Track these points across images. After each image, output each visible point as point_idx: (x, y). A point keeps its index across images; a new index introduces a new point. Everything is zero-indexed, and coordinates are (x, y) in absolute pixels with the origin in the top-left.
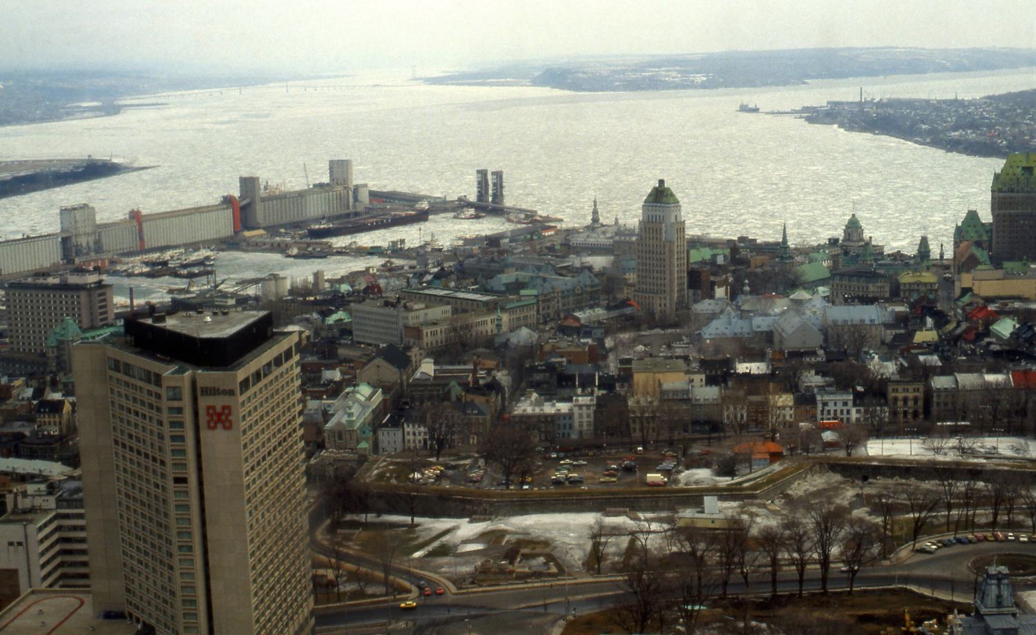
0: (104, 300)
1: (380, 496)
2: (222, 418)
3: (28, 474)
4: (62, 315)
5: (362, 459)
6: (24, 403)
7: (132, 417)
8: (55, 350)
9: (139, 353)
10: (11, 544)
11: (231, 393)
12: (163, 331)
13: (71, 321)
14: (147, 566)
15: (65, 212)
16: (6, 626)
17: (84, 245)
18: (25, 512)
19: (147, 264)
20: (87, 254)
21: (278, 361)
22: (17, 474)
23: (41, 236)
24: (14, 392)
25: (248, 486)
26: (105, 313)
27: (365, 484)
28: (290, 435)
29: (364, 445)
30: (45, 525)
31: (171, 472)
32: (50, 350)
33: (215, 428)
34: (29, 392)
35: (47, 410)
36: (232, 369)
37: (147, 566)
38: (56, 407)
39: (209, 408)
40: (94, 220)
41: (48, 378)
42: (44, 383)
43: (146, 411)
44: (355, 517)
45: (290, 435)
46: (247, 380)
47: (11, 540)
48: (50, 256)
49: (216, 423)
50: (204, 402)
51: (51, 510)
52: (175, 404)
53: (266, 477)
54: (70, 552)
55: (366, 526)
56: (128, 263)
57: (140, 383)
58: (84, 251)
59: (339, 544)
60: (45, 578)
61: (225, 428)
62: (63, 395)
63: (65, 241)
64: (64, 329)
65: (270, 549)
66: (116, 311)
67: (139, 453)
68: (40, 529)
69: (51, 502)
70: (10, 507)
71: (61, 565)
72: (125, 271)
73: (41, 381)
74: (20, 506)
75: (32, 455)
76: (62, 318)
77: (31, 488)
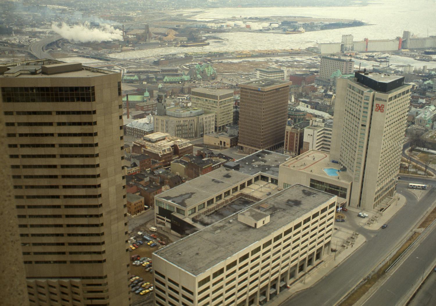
0: (351, 66)
1: (430, 143)
2: (381, 108)
5: (427, 130)
7: (352, 103)
9: (358, 84)
10: (309, 135)
11: (386, 101)
12: (367, 78)
14: (348, 149)
17: (348, 47)
18: (314, 126)
19: (367, 56)
21: (403, 93)
25: (385, 132)
26: (351, 70)
27: (425, 138)
28: (403, 118)
29: (428, 126)
30: (320, 131)
31: (361, 122)
33: (378, 111)
34: (323, 91)
36: (387, 93)
37: (348, 149)
38: (330, 96)
39: (377, 104)
40: (352, 40)
41: (329, 87)
42: (328, 89)
43: (357, 102)
44: (419, 148)
45: (403, 118)
46: (391, 98)
48: (336, 50)
49: (378, 110)
50: (376, 102)
52: (367, 101)
53: (392, 130)
55: (423, 152)
57: (357, 93)
59: (412, 156)
60: (317, 147)
61: (381, 112)
63: (342, 45)
65: (388, 152)
67: (352, 114)
68: (318, 132)
69: (323, 125)
70: (310, 124)
71: (323, 144)
75: (320, 110)
77: (318, 119)
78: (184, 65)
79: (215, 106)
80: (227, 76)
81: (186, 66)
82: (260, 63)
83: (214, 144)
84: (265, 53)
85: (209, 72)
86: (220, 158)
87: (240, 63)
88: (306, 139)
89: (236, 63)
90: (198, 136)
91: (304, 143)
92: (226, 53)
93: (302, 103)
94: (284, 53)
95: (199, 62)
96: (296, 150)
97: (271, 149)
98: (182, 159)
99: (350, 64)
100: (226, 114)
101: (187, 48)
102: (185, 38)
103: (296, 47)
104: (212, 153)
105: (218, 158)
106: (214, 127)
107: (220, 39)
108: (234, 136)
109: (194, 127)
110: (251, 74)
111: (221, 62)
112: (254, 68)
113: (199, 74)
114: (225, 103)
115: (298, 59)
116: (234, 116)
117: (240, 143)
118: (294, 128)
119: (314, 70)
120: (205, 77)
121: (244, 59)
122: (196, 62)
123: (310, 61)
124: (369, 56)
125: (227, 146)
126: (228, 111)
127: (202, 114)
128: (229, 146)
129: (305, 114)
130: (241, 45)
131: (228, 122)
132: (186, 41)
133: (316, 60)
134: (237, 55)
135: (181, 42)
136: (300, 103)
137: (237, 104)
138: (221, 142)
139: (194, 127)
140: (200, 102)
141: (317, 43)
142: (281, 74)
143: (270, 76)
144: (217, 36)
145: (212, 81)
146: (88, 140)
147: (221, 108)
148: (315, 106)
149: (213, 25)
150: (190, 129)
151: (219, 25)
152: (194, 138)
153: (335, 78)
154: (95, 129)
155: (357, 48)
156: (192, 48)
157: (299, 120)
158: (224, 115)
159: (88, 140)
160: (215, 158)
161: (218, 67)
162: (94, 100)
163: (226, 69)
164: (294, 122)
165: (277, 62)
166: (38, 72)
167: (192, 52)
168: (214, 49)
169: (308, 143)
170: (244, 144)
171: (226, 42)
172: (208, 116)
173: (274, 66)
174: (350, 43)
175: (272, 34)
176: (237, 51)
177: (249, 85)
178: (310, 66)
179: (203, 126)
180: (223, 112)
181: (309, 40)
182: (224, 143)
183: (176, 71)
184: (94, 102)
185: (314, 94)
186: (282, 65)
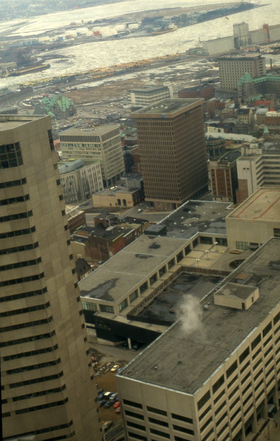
0: (262, 64)
3: (238, 140)
4: (243, 71)
6: (232, 110)
8: (241, 87)
10: (244, 169)
13: (248, 74)
15: (235, 26)
16: (253, 202)
17: (244, 41)
18: (249, 155)
19: (272, 48)
20: (245, 45)
22: (233, 140)
23: (225, 38)
24: (226, 106)
26: (262, 70)
30: (258, 162)
32: (239, 87)
34: (233, 105)
35: (242, 113)
38: (246, 112)
40: (248, 29)
41: (240, 100)
42: (238, 101)
47: (244, 167)
48: (229, 47)
51: (260, 154)
54: (268, 173)
56: (263, 48)
58: (244, 43)
62: (248, 107)
63: (236, 39)
64: (245, 78)
66: (266, 69)
68: (257, 163)
69: (260, 151)
70: (243, 152)
72: (263, 52)
73: (236, 101)
74: (247, 153)
75: (238, 132)
76: (243, 73)
78: (24, 102)
79: (97, 151)
80: (89, 107)
81: (27, 102)
82: (129, 81)
83: (110, 206)
84: (132, 66)
85: (64, 106)
86: (130, 223)
87: (102, 85)
88: (241, 175)
89: (96, 87)
90: (83, 198)
91: (239, 182)
92: (77, 75)
93: (211, 127)
94: (159, 62)
95: (44, 94)
96: (229, 194)
97: (195, 197)
98: (76, 235)
99: (260, 62)
100: (115, 160)
101: (20, 77)
102: (13, 64)
103: (173, 52)
104: (116, 219)
105: (127, 224)
106: (101, 181)
107: (63, 57)
108: (136, 189)
109: (74, 186)
110: (122, 100)
111: (75, 89)
112: (124, 89)
113: (50, 110)
114: (111, 145)
115: (180, 67)
116: (125, 161)
117: (148, 197)
119: (207, 79)
120: (59, 114)
121: (105, 80)
122: (39, 94)
123: (197, 68)
124: (275, 48)
125: (128, 205)
126: (117, 155)
127: (82, 166)
128: (132, 205)
129: (223, 142)
130: (94, 60)
131: (119, 170)
132: (15, 67)
133: (205, 65)
134: (93, 75)
135: (9, 69)
136: (208, 128)
137: (127, 144)
138: (119, 201)
139: (74, 186)
140: (74, 149)
141: (200, 42)
142: (165, 93)
143: (151, 97)
144: (57, 54)
145: (71, 118)
146: (20, 225)
147: (106, 152)
148: (230, 129)
149: (47, 38)
150: (70, 190)
151: (56, 37)
152: (78, 202)
153: (243, 85)
154: (29, 205)
155: (255, 39)
156: (28, 75)
157: (217, 151)
158: (112, 162)
159: (20, 225)
160: (123, 225)
161: (73, 97)
162: (21, 163)
163: (84, 99)
164: (211, 156)
165: (152, 76)
167: (29, 82)
168: (58, 73)
169: (245, 181)
170: (154, 198)
171: (73, 60)
172: (91, 166)
173: (153, 83)
174: (246, 34)
175: (134, 39)
176: (92, 71)
177: (148, 113)
178: (201, 74)
179: (87, 183)
180: (111, 158)
181: (186, 39)
182: (124, 201)
183: (15, 111)
184: (21, 166)
185: (223, 112)
186: (161, 78)
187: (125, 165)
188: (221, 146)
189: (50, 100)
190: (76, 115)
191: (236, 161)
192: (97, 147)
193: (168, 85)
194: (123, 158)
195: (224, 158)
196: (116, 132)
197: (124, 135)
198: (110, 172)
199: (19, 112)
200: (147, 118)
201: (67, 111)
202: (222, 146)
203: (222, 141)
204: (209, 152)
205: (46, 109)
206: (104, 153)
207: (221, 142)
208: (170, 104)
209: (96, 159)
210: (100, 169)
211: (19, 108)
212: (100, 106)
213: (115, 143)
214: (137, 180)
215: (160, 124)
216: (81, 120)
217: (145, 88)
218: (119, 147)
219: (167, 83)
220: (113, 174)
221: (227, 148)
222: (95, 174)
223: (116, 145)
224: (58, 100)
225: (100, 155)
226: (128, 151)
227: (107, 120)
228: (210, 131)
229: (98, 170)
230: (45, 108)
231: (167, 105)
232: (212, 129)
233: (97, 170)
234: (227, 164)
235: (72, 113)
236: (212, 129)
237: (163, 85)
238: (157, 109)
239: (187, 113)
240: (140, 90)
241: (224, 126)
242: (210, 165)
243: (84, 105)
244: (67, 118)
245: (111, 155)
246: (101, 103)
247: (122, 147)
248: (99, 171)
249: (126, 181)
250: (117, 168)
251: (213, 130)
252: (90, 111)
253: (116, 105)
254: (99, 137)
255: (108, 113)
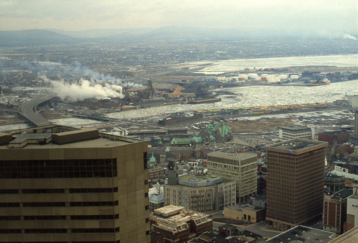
10: (353, 206)
16: (351, 236)
78: (194, 125)
79: (236, 172)
80: (244, 136)
81: (196, 125)
82: (281, 120)
83: (237, 219)
84: (286, 108)
85: (223, 132)
86: (246, 236)
87: (259, 120)
88: (350, 211)
89: (253, 121)
90: (217, 209)
91: (347, 216)
92: (241, 110)
93: (338, 167)
94: (308, 107)
95: (211, 121)
96: (338, 225)
97: (308, 224)
98: (201, 238)
100: (249, 182)
102: (193, 94)
103: (322, 101)
104: (237, 230)
105: (244, 236)
106: (235, 197)
107: (233, 94)
108: (261, 208)
109: (211, 198)
110: (272, 134)
111: (237, 120)
112: (275, 126)
113: (212, 134)
114: (248, 170)
116: (258, 184)
117: (269, 217)
118: (334, 197)
119: (346, 126)
120: (218, 138)
121: (262, 117)
122: (207, 121)
123: (340, 116)
125: (252, 221)
126: (252, 178)
127: (220, 183)
128: (255, 221)
129: (343, 179)
130: (257, 100)
131: (252, 191)
132: (194, 97)
133: (347, 115)
134: (254, 112)
135: (188, 98)
136: (336, 166)
137: (261, 170)
138: (245, 216)
139: (211, 198)
140: (218, 168)
141: (346, 96)
142: (307, 133)
143: (295, 135)
144: (229, 91)
145: (227, 143)
146: (107, 224)
147: (242, 175)
149: (224, 78)
150: (207, 201)
151: (231, 78)
152: (212, 211)
154: (116, 210)
157: (337, 187)
158: (247, 183)
159: (107, 224)
160: (240, 236)
162: (116, 175)
164: (331, 190)
165: (301, 118)
166: (48, 141)
168: (226, 106)
170: (273, 218)
171: (240, 97)
172: (228, 184)
173: (299, 123)
175: (292, 87)
176: (253, 107)
177: (278, 147)
178: (341, 122)
179: (223, 197)
181: (336, 92)
182: (249, 217)
183: (185, 131)
184: (114, 178)
185: (351, 155)
186: (308, 120)
187: (257, 187)
188: (341, 183)
189: (214, 126)
190: (232, 141)
191: (347, 199)
192: (236, 169)
193: (311, 127)
194: (256, 181)
195: (337, 194)
196: (254, 159)
197: (262, 163)
198: (243, 191)
199: (188, 132)
200: (276, 152)
201: (225, 136)
202: (342, 184)
203: (342, 179)
204: (330, 186)
205: (209, 133)
206: (241, 175)
207: (342, 180)
208: (298, 143)
209: (234, 179)
210: (235, 187)
211: (189, 129)
212: (253, 136)
213: (251, 169)
214: (263, 201)
215: (287, 158)
216: (235, 146)
217: (292, 127)
218: (254, 172)
219: (311, 125)
220: (246, 193)
221: (346, 186)
222: (231, 191)
223: (252, 170)
224: (219, 127)
225: (238, 176)
226: (262, 176)
227: (256, 148)
228: (337, 170)
229: (230, 189)
230: (209, 132)
231: (295, 143)
232: (338, 168)
233: (232, 188)
234: (339, 199)
235: (229, 139)
236: (338, 168)
237: (307, 127)
238: (287, 145)
239: (311, 153)
240: (287, 128)
241: (349, 167)
242: (325, 198)
243: (241, 133)
244: (224, 142)
245: (246, 177)
246: (254, 134)
247: (258, 173)
248: (234, 189)
249: (254, 201)
250: (250, 189)
251: (339, 169)
252: (244, 139)
253: (266, 138)
254: (238, 161)
255: (258, 143)
